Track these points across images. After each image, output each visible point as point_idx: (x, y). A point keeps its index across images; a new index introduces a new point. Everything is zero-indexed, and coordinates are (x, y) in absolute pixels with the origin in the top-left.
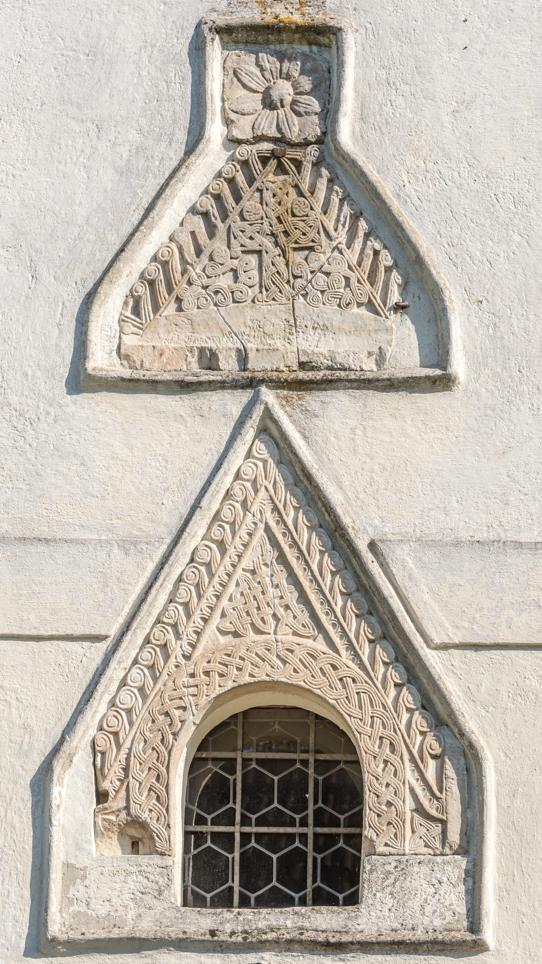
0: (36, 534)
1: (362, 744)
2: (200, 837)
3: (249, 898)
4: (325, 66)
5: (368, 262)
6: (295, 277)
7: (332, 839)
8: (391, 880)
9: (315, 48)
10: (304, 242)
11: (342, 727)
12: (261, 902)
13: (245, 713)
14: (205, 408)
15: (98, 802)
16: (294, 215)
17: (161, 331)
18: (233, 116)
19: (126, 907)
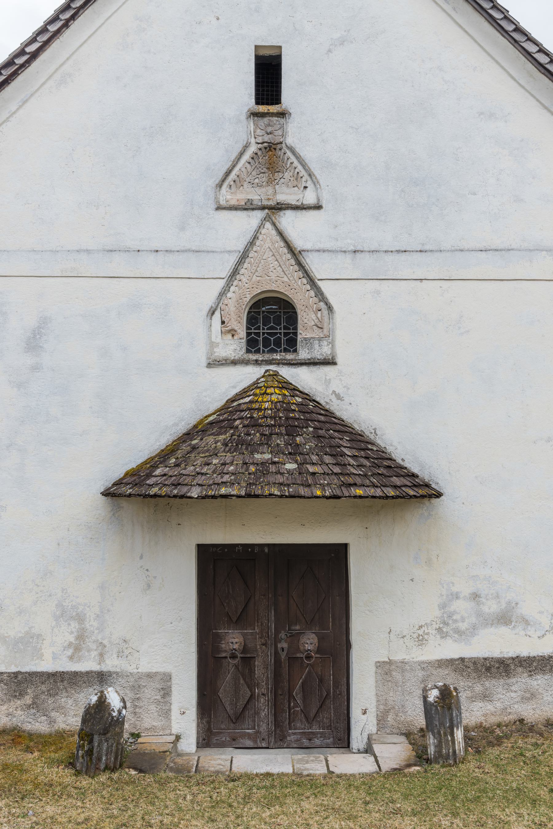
0: (203, 250)
1: (298, 307)
2: (251, 333)
3: (265, 351)
4: (282, 123)
5: (295, 175)
6: (275, 180)
7: (289, 333)
8: (308, 345)
9: (279, 118)
10: (277, 170)
11: (291, 302)
12: (269, 352)
13: (263, 299)
14: (251, 215)
15: (222, 324)
16: (274, 163)
17: (238, 194)
18: (256, 136)
19: (231, 354)
